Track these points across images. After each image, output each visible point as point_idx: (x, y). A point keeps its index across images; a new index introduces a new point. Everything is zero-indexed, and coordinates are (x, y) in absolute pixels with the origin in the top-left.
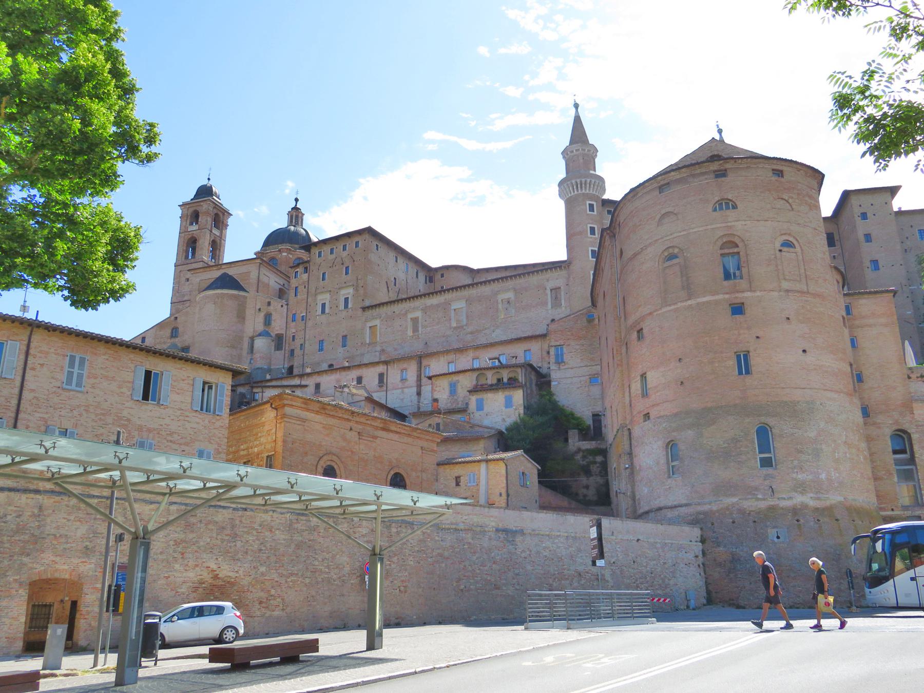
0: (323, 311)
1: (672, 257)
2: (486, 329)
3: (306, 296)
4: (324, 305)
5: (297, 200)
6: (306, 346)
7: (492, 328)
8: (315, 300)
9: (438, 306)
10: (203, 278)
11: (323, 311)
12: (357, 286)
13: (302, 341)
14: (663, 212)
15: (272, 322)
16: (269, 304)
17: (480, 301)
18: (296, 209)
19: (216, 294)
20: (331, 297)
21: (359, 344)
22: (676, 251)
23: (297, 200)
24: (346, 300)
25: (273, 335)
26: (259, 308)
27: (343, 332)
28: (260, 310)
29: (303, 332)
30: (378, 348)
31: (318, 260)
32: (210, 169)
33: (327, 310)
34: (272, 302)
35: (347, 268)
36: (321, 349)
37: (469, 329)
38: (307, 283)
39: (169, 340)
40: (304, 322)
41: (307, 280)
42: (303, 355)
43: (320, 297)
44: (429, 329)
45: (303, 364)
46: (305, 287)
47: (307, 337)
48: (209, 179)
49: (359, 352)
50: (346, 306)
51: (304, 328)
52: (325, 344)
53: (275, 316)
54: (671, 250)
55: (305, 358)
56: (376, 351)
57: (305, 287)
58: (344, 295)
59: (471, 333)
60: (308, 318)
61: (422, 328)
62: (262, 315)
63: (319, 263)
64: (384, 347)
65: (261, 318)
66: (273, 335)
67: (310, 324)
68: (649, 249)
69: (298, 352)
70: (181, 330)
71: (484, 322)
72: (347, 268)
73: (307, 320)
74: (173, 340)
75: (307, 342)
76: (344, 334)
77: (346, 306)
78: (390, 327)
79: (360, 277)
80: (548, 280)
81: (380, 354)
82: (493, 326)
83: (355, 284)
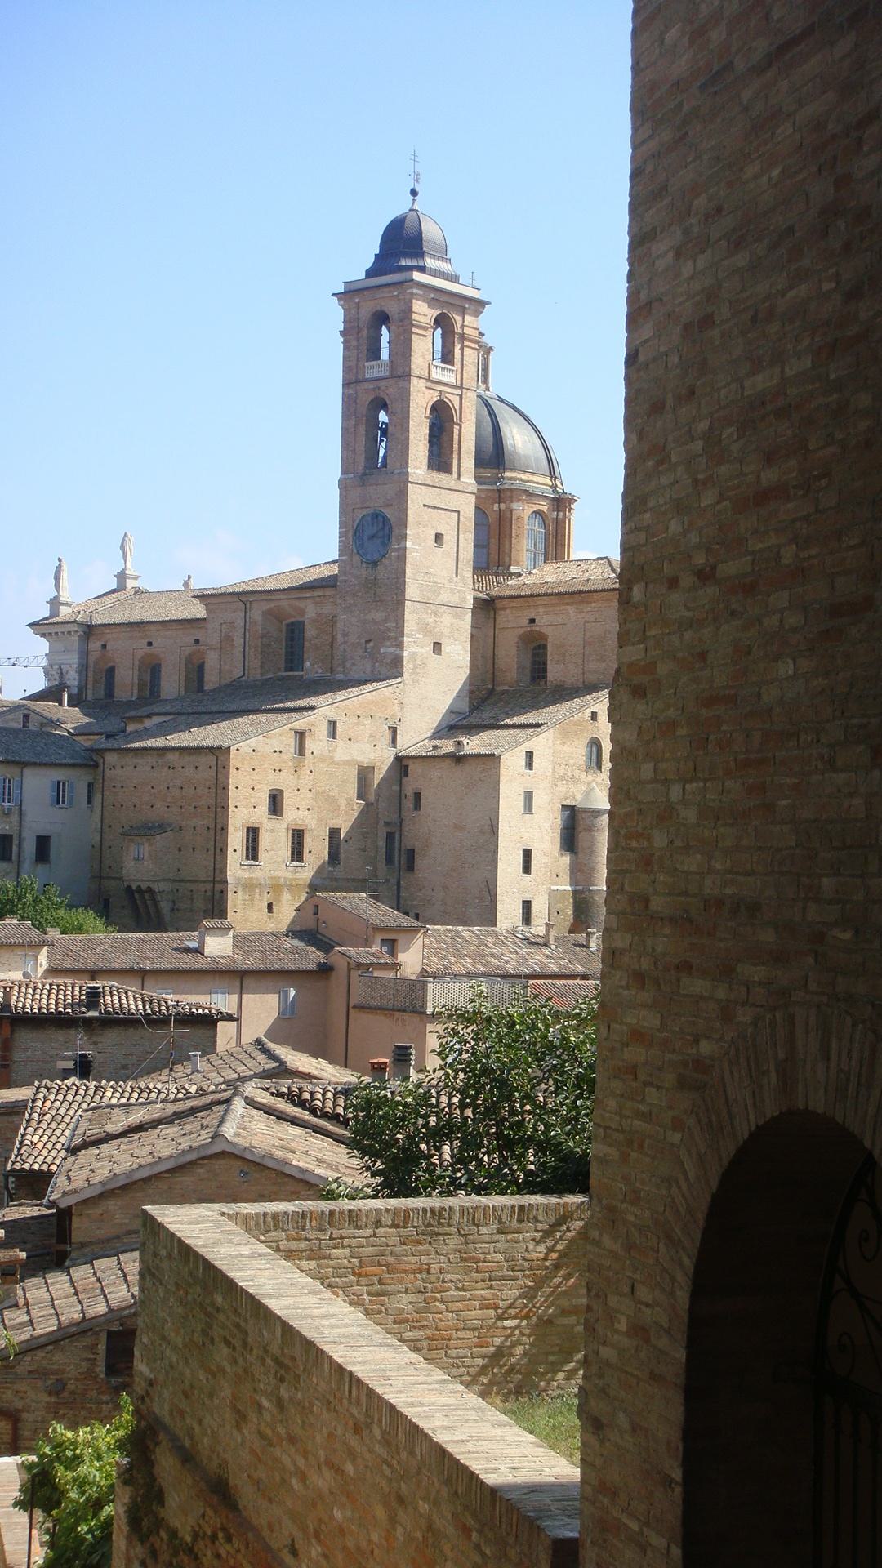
48: (414, 193)
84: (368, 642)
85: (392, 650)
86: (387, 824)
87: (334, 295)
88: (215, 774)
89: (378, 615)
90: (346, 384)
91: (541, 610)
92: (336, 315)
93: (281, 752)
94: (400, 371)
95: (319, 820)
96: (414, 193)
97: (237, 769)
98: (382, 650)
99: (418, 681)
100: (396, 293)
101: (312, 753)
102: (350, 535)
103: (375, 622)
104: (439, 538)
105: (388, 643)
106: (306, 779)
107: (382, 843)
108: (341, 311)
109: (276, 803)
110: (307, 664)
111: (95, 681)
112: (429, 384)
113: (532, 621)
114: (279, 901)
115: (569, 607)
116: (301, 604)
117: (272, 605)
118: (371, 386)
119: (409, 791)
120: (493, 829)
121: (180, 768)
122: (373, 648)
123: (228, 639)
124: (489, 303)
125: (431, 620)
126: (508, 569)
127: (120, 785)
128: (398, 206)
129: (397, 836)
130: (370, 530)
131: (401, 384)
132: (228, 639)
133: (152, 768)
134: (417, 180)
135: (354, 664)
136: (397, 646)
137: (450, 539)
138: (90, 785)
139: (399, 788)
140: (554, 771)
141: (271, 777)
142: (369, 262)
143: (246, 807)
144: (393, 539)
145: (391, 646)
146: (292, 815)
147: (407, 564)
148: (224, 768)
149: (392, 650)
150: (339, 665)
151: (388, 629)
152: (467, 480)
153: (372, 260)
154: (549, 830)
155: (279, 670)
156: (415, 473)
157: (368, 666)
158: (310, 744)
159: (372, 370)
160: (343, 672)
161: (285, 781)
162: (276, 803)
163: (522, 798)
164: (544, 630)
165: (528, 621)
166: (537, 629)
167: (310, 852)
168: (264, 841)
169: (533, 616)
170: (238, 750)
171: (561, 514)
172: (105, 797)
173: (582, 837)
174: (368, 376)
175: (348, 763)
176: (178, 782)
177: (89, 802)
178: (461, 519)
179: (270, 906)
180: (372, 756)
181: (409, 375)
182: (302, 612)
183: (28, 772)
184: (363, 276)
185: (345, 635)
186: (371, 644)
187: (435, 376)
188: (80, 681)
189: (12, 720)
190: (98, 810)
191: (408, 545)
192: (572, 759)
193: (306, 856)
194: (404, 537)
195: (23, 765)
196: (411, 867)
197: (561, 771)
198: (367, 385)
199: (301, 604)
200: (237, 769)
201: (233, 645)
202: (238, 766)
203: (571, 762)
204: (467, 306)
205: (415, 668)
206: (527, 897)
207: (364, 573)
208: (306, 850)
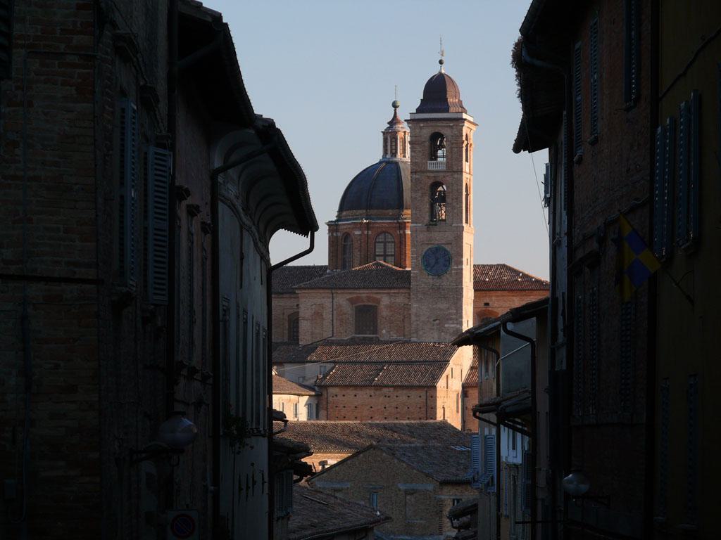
5: (395, 106)
48: (441, 62)
85: (453, 326)
88: (425, 401)
89: (443, 305)
91: (493, 298)
96: (441, 62)
98: (446, 326)
100: (451, 125)
102: (420, 259)
103: (441, 310)
105: (451, 322)
113: (487, 304)
115: (514, 298)
116: (378, 296)
117: (355, 295)
118: (432, 175)
121: (395, 397)
122: (438, 325)
127: (342, 406)
128: (434, 71)
130: (432, 261)
131: (456, 176)
133: (371, 396)
134: (442, 55)
135: (424, 333)
136: (457, 324)
144: (453, 264)
145: (453, 323)
148: (432, 397)
149: (453, 326)
150: (414, 333)
151: (450, 314)
157: (436, 336)
159: (431, 166)
160: (417, 337)
165: (483, 304)
166: (490, 309)
169: (487, 300)
172: (329, 413)
174: (429, 169)
176: (394, 404)
181: (462, 172)
182: (378, 301)
185: (417, 315)
186: (437, 322)
198: (428, 174)
199: (378, 296)
201: (323, 319)
207: (431, 281)
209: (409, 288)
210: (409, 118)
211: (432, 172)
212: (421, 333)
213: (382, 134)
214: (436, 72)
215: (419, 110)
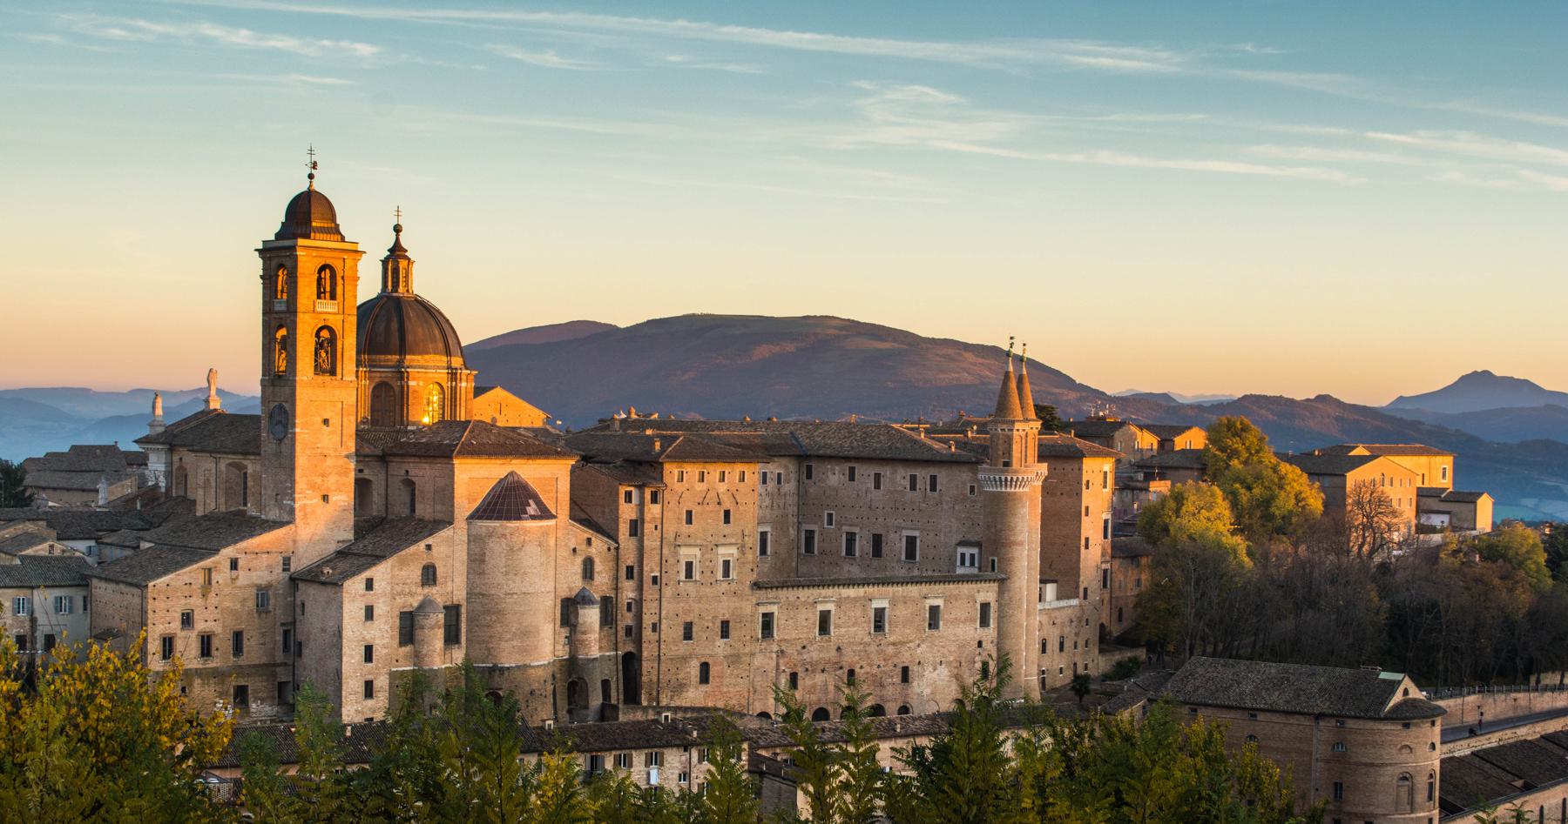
0: (689, 574)
1: (1405, 779)
2: (910, 642)
3: (659, 543)
4: (689, 565)
5: (397, 229)
6: (662, 627)
7: (917, 642)
8: (676, 554)
9: (856, 599)
10: (474, 474)
11: (689, 574)
12: (743, 546)
13: (655, 619)
14: (1403, 743)
15: (596, 575)
16: (589, 541)
17: (905, 603)
18: (397, 252)
19: (541, 527)
20: (703, 555)
21: (748, 638)
22: (1408, 776)
23: (397, 229)
24: (727, 564)
25: (597, 597)
26: (573, 547)
27: (724, 615)
28: (574, 550)
29: (656, 604)
30: (775, 648)
31: (679, 487)
32: (311, 152)
33: (697, 575)
34: (593, 539)
35: (727, 513)
36: (688, 635)
37: (891, 639)
38: (660, 521)
39: (419, 590)
40: (658, 587)
41: (660, 516)
42: (659, 641)
43: (683, 551)
44: (843, 630)
45: (659, 655)
46: (656, 528)
47: (664, 613)
48: (311, 176)
49: (747, 650)
50: (726, 573)
51: (657, 596)
52: (694, 629)
53: (598, 567)
54: (1405, 774)
55: (662, 646)
56: (771, 652)
57: (656, 528)
58: (723, 555)
59: (894, 644)
60: (664, 581)
61: (835, 628)
62: (579, 560)
63: (680, 491)
64: (783, 648)
65: (577, 566)
66: (597, 597)
67: (668, 592)
68: (1389, 768)
69: (648, 634)
70: (440, 571)
71: (908, 631)
72: (727, 513)
73: (663, 585)
74: (427, 590)
75: (664, 621)
76: (725, 618)
77: (726, 573)
78: (792, 618)
79: (746, 533)
80: (978, 591)
81: (778, 656)
82: (919, 639)
83: (739, 541)
84: (277, 495)
85: (289, 502)
86: (283, 624)
87: (256, 250)
90: (264, 313)
92: (258, 264)
93: (190, 584)
94: (291, 310)
95: (224, 626)
97: (154, 599)
99: (308, 524)
100: (288, 254)
101: (218, 582)
104: (326, 422)
105: (287, 498)
106: (213, 600)
107: (280, 638)
108: (261, 261)
109: (187, 620)
110: (249, 505)
111: (177, 483)
112: (314, 315)
114: (191, 685)
116: (245, 462)
119: (298, 602)
120: (339, 634)
123: (207, 481)
124: (365, 252)
125: (319, 480)
126: (406, 428)
129: (292, 632)
132: (207, 481)
135: (270, 510)
137: (335, 421)
138: (85, 598)
139: (292, 599)
140: (392, 589)
141: (183, 601)
142: (277, 228)
143: (163, 624)
146: (200, 626)
147: (297, 444)
151: (287, 487)
152: (350, 379)
153: (279, 226)
154: (389, 630)
155: (240, 504)
156: (302, 380)
158: (215, 577)
161: (196, 602)
162: (187, 620)
163: (363, 611)
164: (414, 479)
167: (217, 649)
168: (179, 645)
170: (154, 586)
171: (454, 383)
173: (419, 634)
175: (248, 586)
177: (85, 609)
178: (344, 406)
179: (183, 690)
180: (269, 579)
183: (35, 592)
184: (273, 238)
187: (318, 309)
188: (167, 483)
189: (41, 549)
190: (89, 615)
191: (298, 430)
192: (409, 579)
193: (214, 653)
194: (294, 425)
195: (32, 588)
196: (300, 655)
197: (399, 589)
199: (245, 462)
200: (154, 599)
202: (156, 596)
203: (408, 581)
204: (345, 257)
205: (305, 515)
206: (370, 677)
208: (214, 648)
209: (259, 454)
210: (261, 247)
211: (277, 313)
212: (267, 509)
213: (381, 263)
214: (304, 188)
215: (279, 236)
